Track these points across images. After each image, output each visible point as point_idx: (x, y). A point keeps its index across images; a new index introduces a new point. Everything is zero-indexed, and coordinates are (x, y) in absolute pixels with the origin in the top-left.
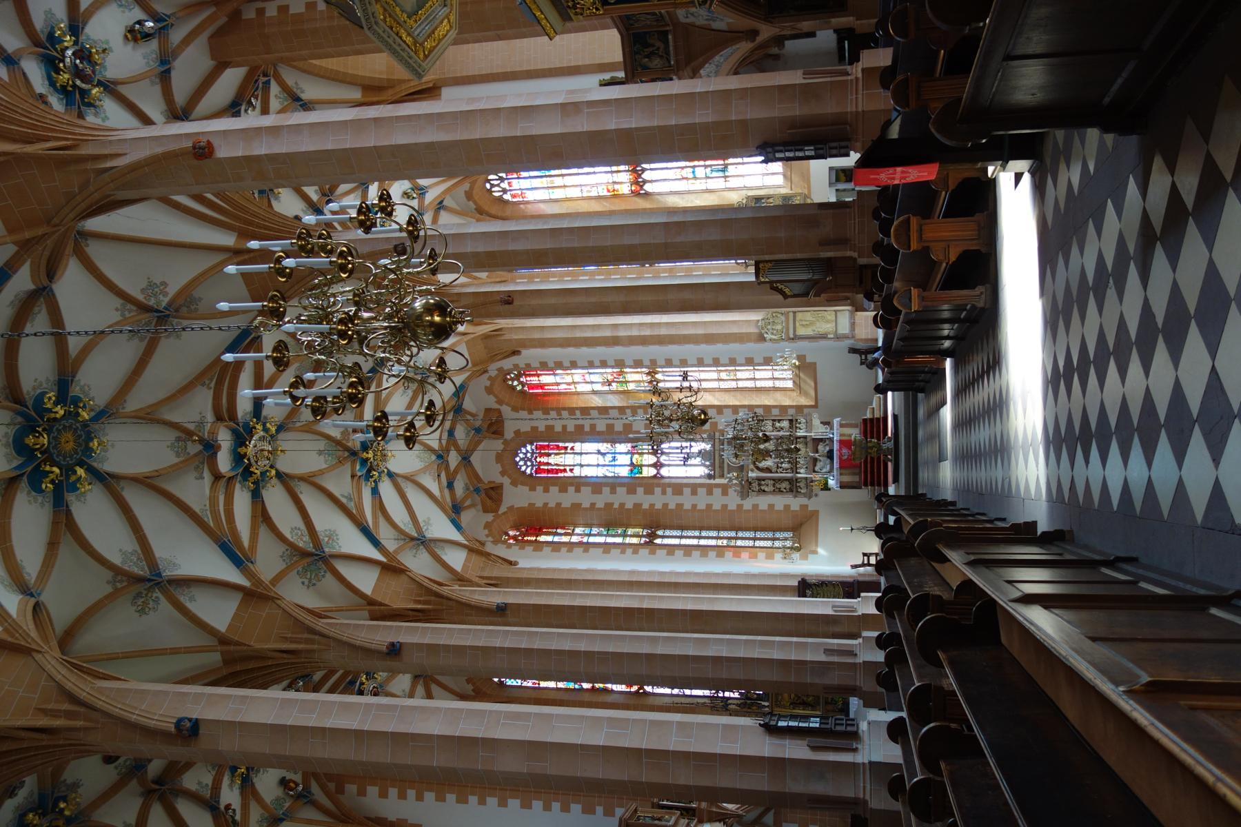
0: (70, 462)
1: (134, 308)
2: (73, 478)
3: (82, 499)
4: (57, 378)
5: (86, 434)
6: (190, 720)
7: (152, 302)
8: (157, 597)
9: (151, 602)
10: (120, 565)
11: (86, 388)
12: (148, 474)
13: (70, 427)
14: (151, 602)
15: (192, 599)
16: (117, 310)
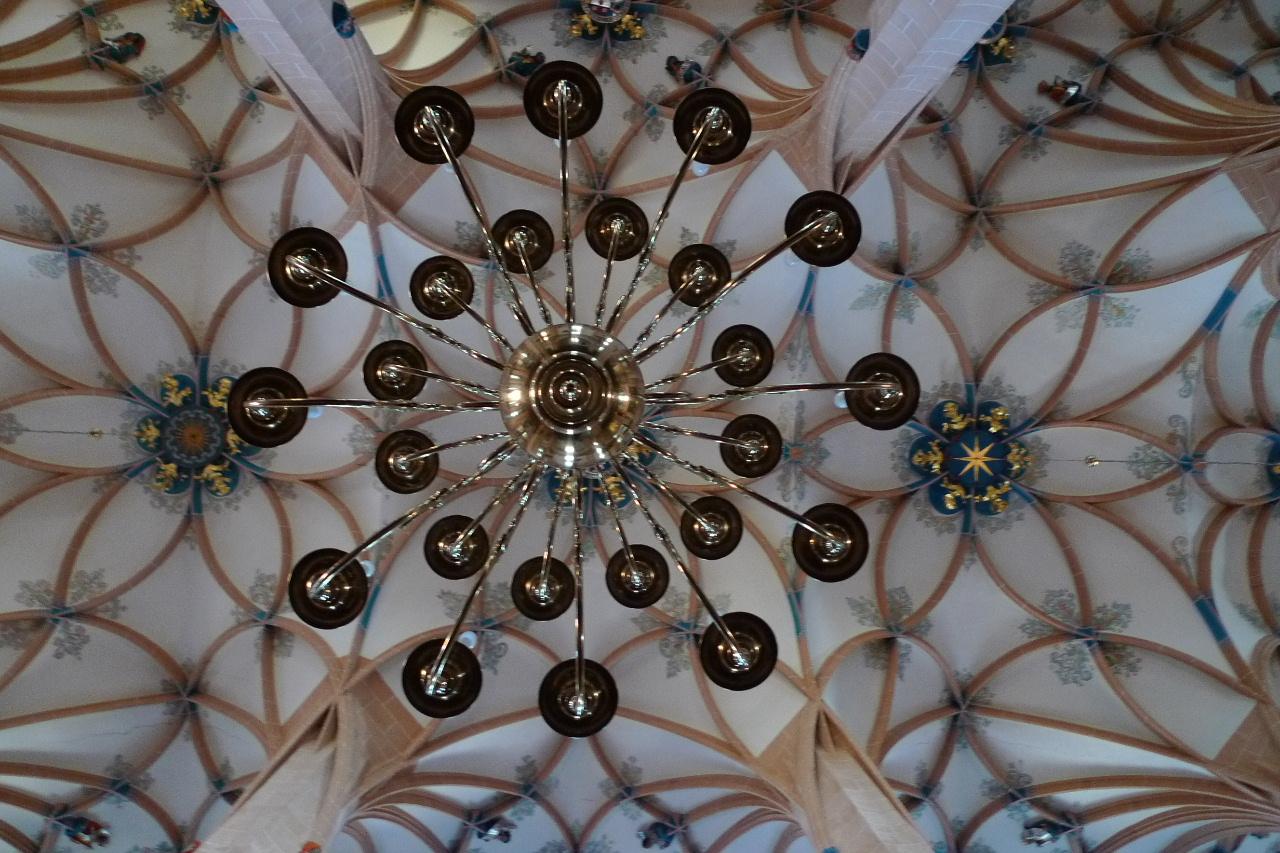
0: (188, 412)
1: (100, 615)
2: (184, 393)
3: (163, 366)
4: (205, 514)
5: (161, 450)
6: (339, 31)
7: (74, 624)
8: (75, 225)
9: (82, 220)
10: (121, 275)
11: (157, 503)
12: (64, 392)
13: (189, 455)
14: (82, 220)
15: (22, 210)
16: (124, 608)
